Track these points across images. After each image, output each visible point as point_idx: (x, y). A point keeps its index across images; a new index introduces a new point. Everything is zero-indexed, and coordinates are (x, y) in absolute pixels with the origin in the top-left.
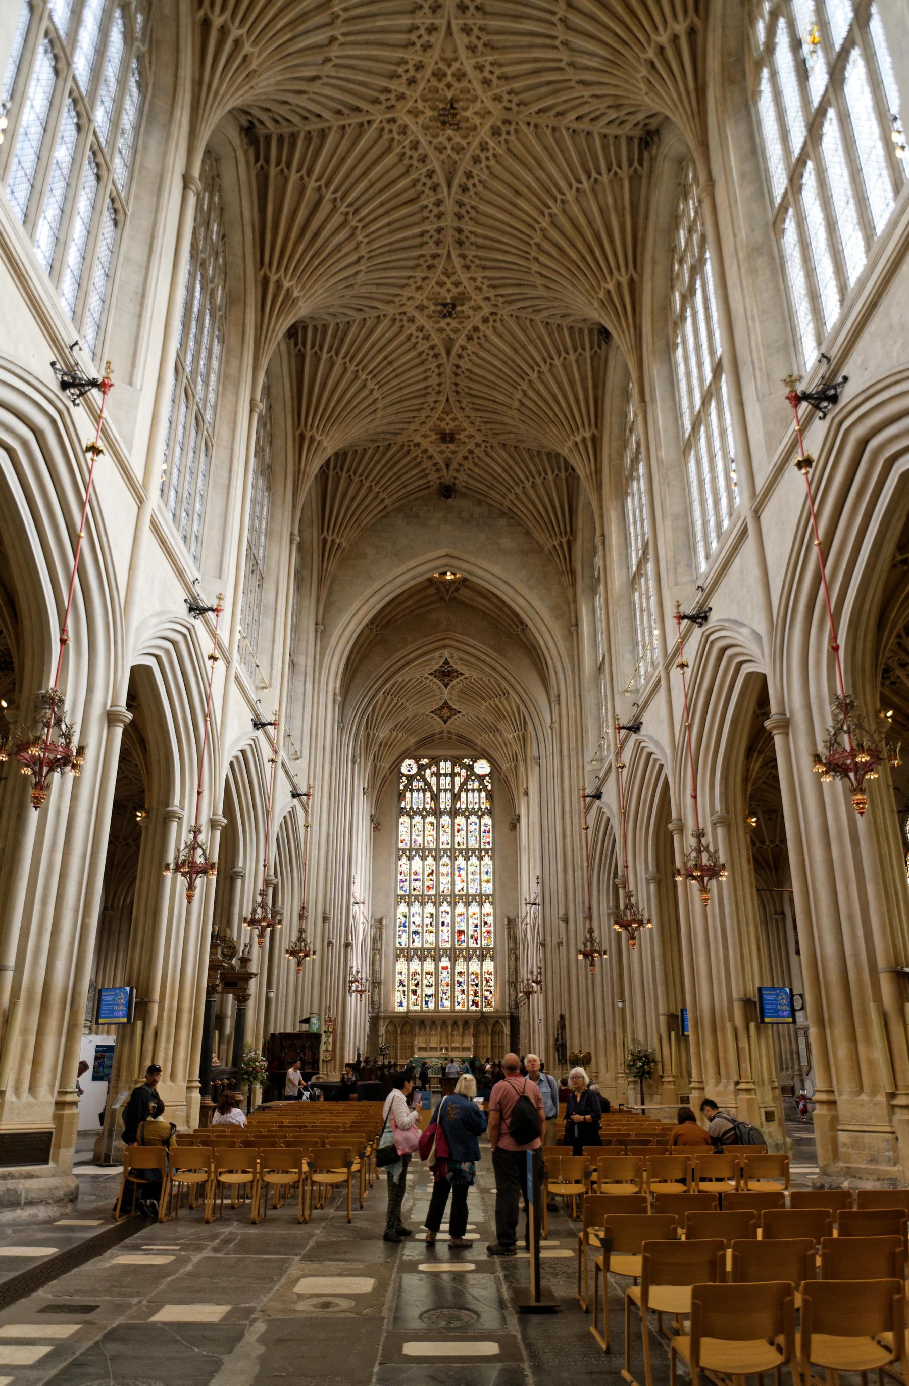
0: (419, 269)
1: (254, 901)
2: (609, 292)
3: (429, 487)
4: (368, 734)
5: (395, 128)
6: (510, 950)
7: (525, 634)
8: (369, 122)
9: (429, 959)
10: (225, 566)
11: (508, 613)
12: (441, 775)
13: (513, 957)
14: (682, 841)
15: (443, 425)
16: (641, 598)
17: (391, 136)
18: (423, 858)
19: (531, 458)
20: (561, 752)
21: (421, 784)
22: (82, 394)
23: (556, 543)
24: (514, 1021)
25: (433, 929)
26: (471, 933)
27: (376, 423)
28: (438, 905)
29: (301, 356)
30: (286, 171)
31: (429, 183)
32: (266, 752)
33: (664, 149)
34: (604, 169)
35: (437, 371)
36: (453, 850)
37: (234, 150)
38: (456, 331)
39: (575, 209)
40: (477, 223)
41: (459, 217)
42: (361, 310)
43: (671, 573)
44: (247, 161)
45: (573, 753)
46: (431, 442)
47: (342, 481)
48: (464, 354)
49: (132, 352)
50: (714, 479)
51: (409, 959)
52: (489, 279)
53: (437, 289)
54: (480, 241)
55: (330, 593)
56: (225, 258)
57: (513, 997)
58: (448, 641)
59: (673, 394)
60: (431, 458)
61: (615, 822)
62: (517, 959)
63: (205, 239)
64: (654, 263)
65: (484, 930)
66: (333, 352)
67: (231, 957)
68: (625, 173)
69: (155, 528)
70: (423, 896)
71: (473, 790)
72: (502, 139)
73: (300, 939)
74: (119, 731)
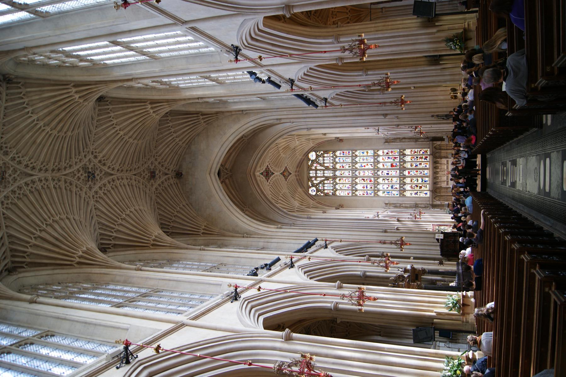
0: (72, 189)
1: (377, 266)
2: (80, 97)
3: (177, 183)
4: (297, 211)
5: (6, 202)
6: (400, 142)
7: (248, 135)
8: (3, 214)
9: (405, 181)
10: (215, 282)
11: (237, 144)
12: (316, 176)
13: (404, 140)
14: (347, 58)
15: (147, 177)
16: (228, 80)
17: (10, 204)
18: (356, 184)
19: (162, 134)
20: (305, 118)
21: (321, 185)
22: (132, 354)
23: (203, 121)
25: (390, 179)
27: (146, 209)
29: (115, 246)
30: (27, 254)
31: (31, 185)
32: (305, 261)
33: (12, 72)
34: (21, 101)
35: (121, 180)
36: (352, 170)
37: (19, 278)
38: (101, 171)
39: (41, 114)
40: (49, 161)
41: (46, 170)
42: (92, 217)
43: (215, 65)
44: (24, 272)
45: (305, 112)
46: (155, 182)
47: (174, 225)
48: (112, 167)
49: (112, 329)
50: (169, 44)
51: (405, 190)
52: (75, 155)
53: (81, 180)
54: (58, 160)
55: (229, 231)
56: (69, 283)
57: (423, 140)
58: (251, 173)
59: (128, 65)
60: (162, 183)
61: (338, 91)
62: (404, 138)
63: (60, 292)
64: (65, 76)
65: (391, 154)
66: (113, 230)
67: (404, 277)
68: (24, 90)
69: (196, 318)
70: (374, 184)
71: (324, 160)
72: (9, 150)
73: (396, 244)
74: (295, 335)
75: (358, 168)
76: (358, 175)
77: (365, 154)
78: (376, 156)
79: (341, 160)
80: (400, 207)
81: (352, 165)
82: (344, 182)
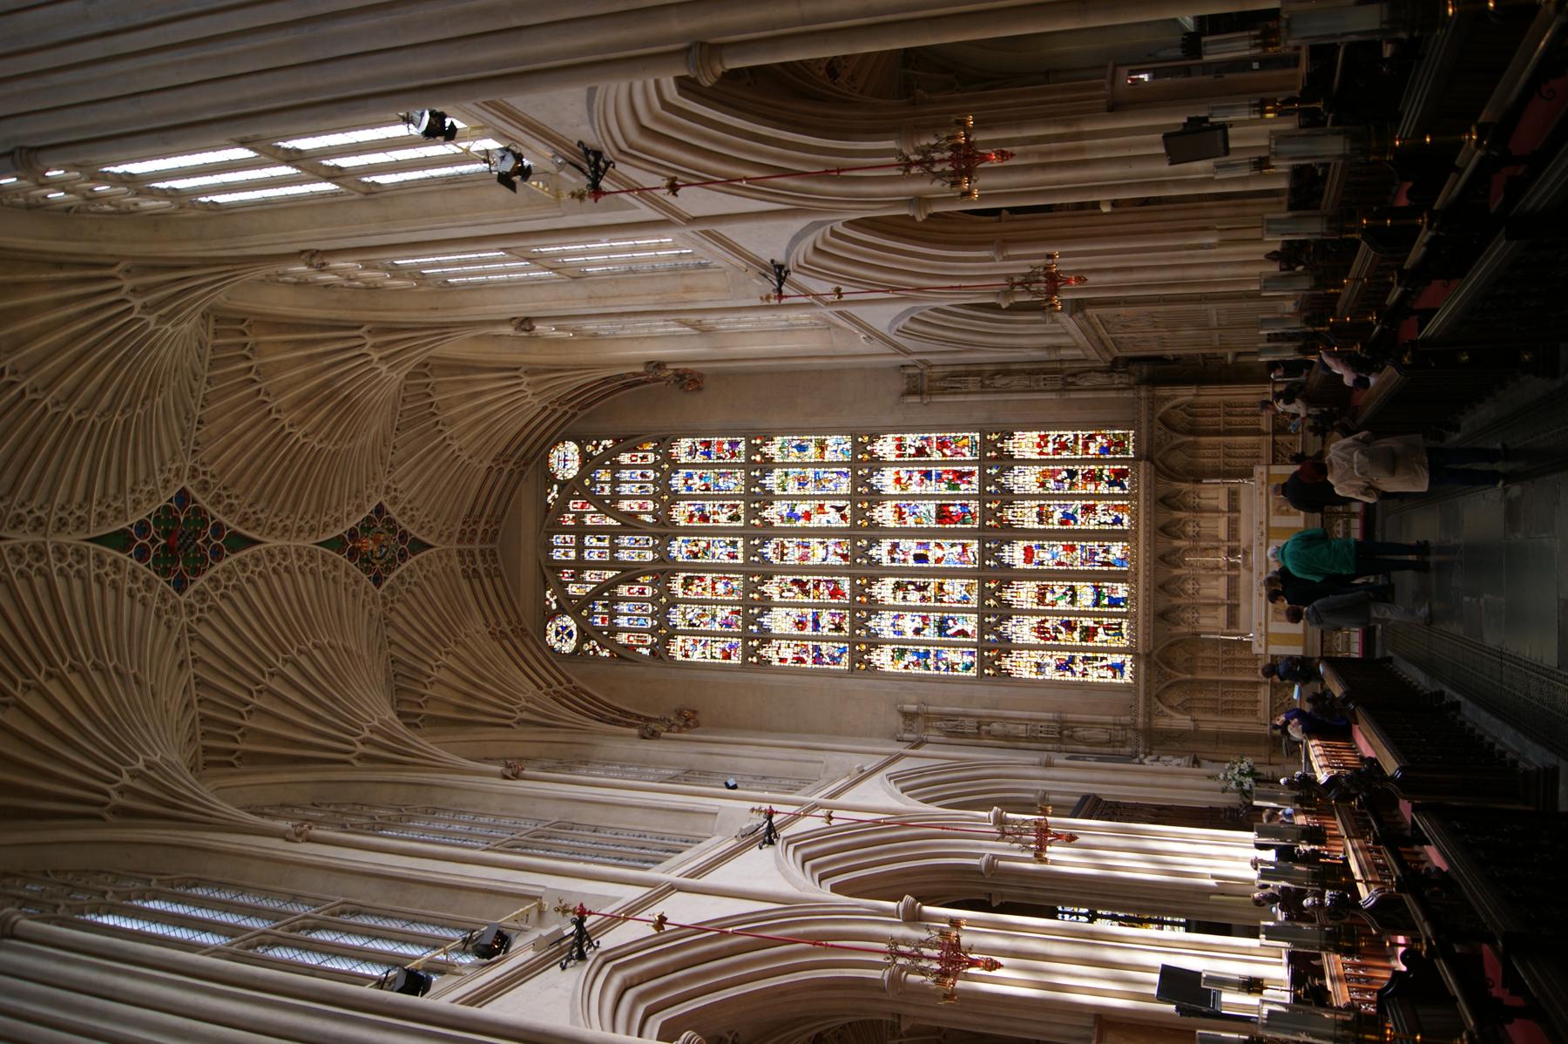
6: (984, 389)
9: (1007, 595)
13: (1000, 381)
18: (767, 605)
26: (943, 488)
28: (875, 572)
51: (1006, 646)
57: (1100, 379)
62: (1005, 370)
65: (937, 456)
70: (853, 608)
71: (615, 482)
75: (777, 523)
77: (812, 451)
78: (864, 464)
80: (978, 735)
81: (748, 509)
82: (708, 595)
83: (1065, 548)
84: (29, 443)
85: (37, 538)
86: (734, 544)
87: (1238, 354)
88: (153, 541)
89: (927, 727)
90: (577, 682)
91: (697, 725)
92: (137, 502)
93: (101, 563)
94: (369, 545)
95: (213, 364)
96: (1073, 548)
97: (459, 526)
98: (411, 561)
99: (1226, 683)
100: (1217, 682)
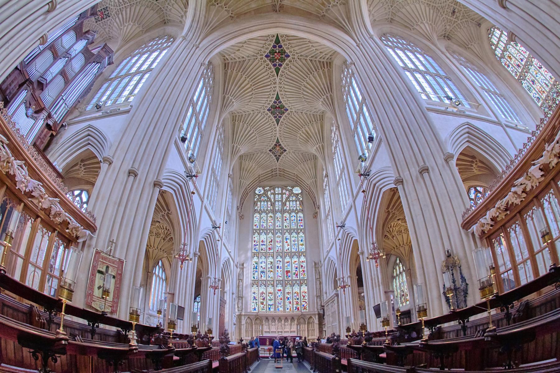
9: (270, 286)
13: (318, 282)
24: (321, 317)
25: (273, 270)
57: (319, 304)
62: (320, 283)
65: (301, 270)
71: (293, 201)
75: (285, 236)
76: (276, 236)
77: (301, 243)
78: (299, 254)
79: (293, 218)
80: (239, 280)
82: (268, 221)
83: (281, 298)
84: (296, 80)
85: (278, 83)
86: (280, 226)
87: (325, 331)
88: (278, 104)
89: (240, 268)
90: (249, 194)
91: (240, 219)
92: (285, 101)
93: (273, 95)
94: (278, 148)
95: (313, 115)
96: (281, 299)
97: (282, 168)
98: (275, 158)
99: (252, 331)
100: (252, 329)
